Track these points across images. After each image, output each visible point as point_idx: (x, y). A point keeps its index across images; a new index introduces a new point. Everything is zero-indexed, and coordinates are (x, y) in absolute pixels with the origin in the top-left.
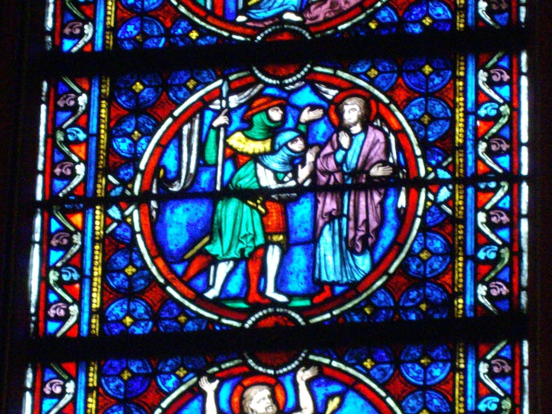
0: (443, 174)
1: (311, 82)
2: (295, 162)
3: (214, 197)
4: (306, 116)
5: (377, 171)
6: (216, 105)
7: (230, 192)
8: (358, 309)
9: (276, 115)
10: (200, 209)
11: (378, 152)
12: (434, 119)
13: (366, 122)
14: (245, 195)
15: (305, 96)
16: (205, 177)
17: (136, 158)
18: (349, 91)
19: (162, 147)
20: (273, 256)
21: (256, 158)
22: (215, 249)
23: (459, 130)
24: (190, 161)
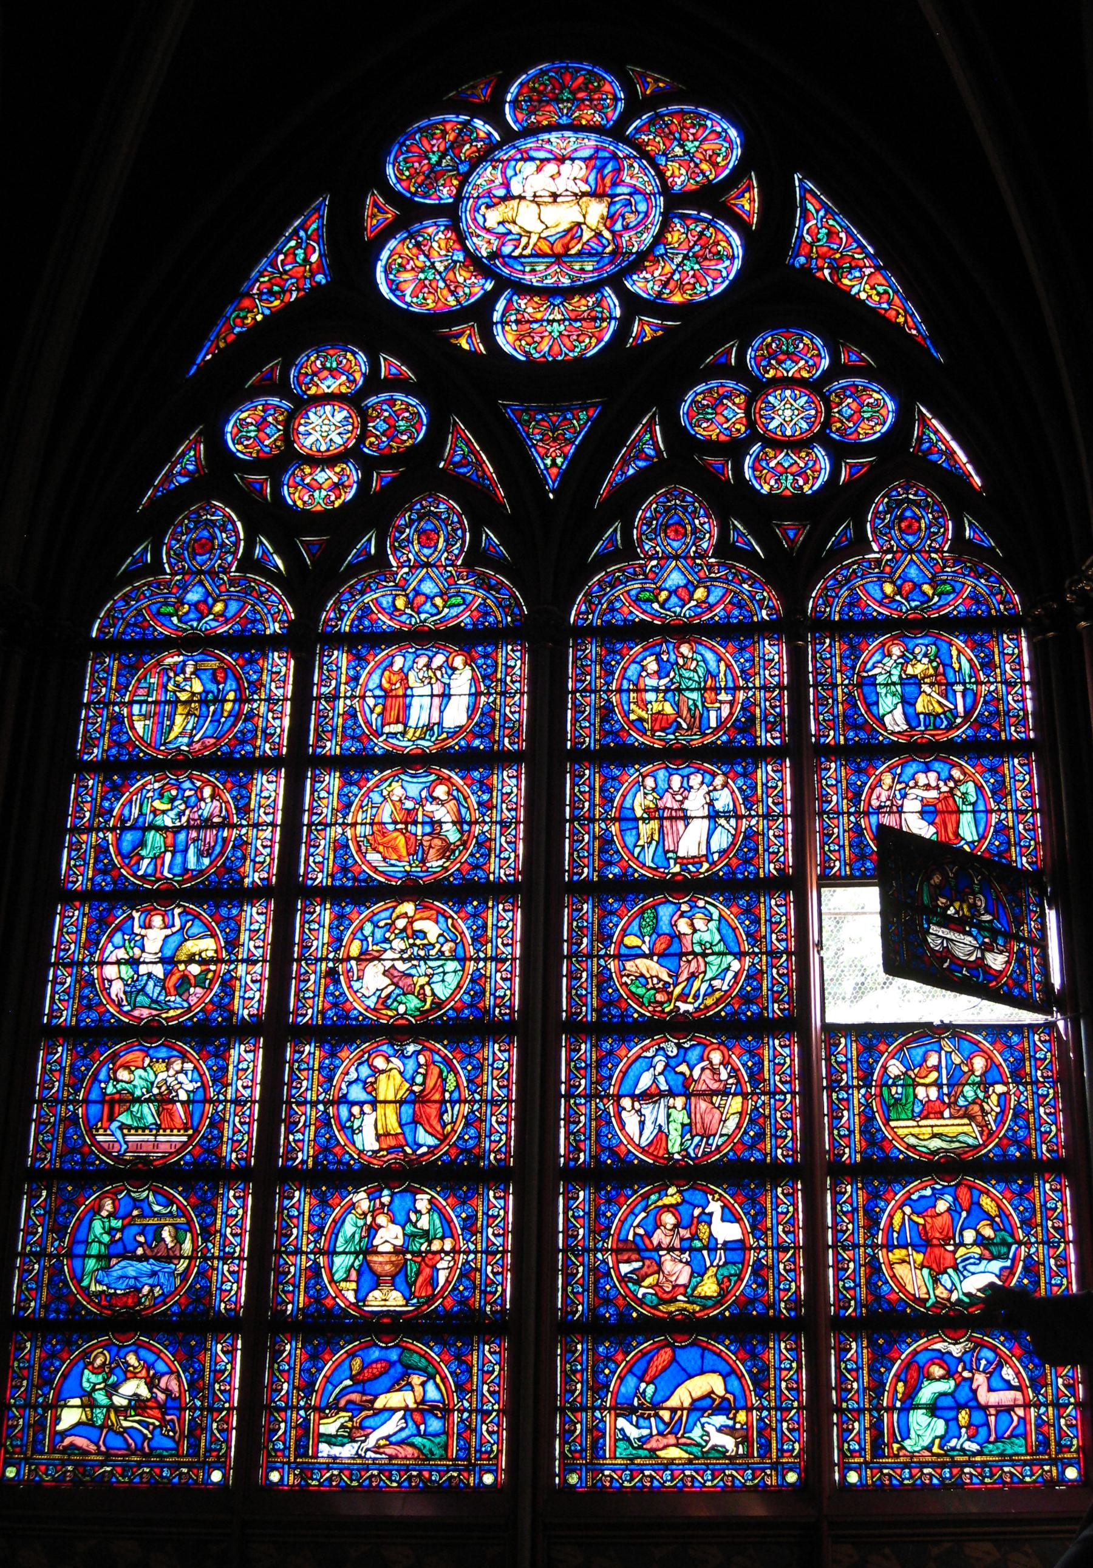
0: (244, 822)
1: (190, 778)
2: (180, 815)
3: (145, 829)
4: (187, 793)
5: (216, 820)
6: (149, 787)
7: (153, 827)
8: (202, 882)
9: (174, 792)
10: (139, 834)
11: (217, 812)
12: (242, 797)
13: (213, 797)
14: (158, 829)
15: (187, 785)
16: (141, 820)
17: (112, 810)
18: (207, 783)
19: (123, 805)
20: (168, 856)
21: (164, 812)
22: (143, 853)
23: (253, 803)
24: (135, 812)
